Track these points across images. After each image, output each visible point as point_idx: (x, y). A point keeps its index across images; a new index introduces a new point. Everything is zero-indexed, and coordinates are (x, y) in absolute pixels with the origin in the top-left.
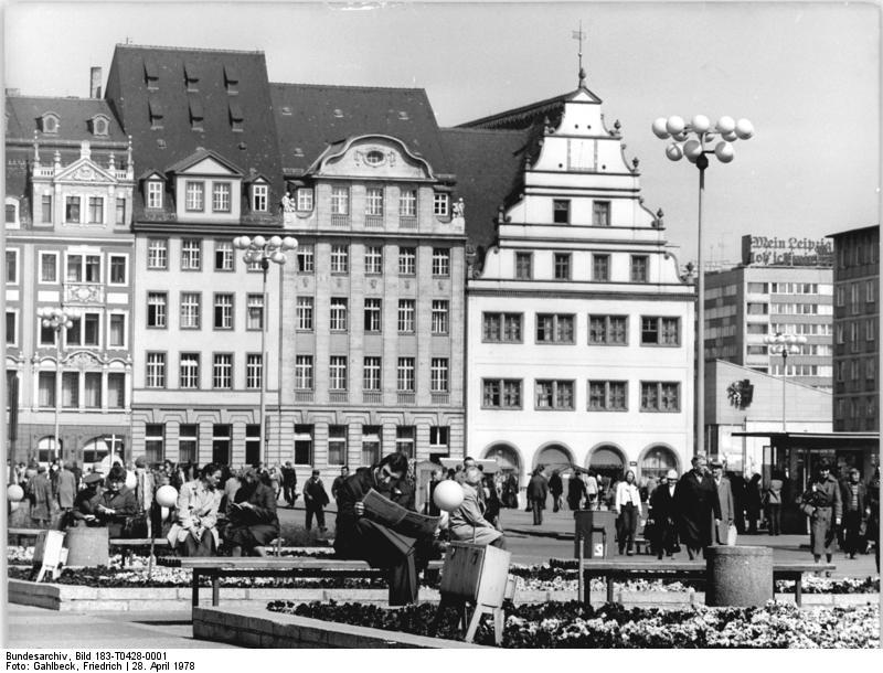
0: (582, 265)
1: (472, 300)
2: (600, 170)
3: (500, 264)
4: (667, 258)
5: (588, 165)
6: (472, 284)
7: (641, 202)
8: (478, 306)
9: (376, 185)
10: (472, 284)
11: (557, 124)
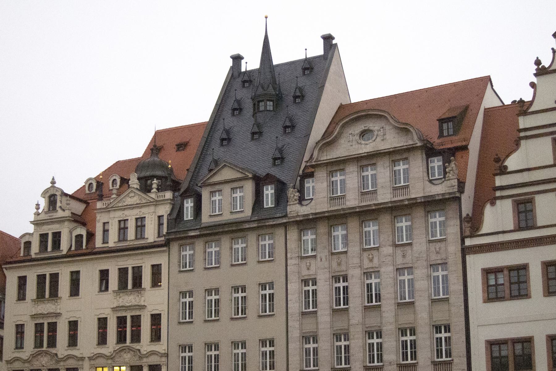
1: (470, 259)
3: (498, 217)
6: (468, 242)
8: (477, 263)
10: (468, 242)
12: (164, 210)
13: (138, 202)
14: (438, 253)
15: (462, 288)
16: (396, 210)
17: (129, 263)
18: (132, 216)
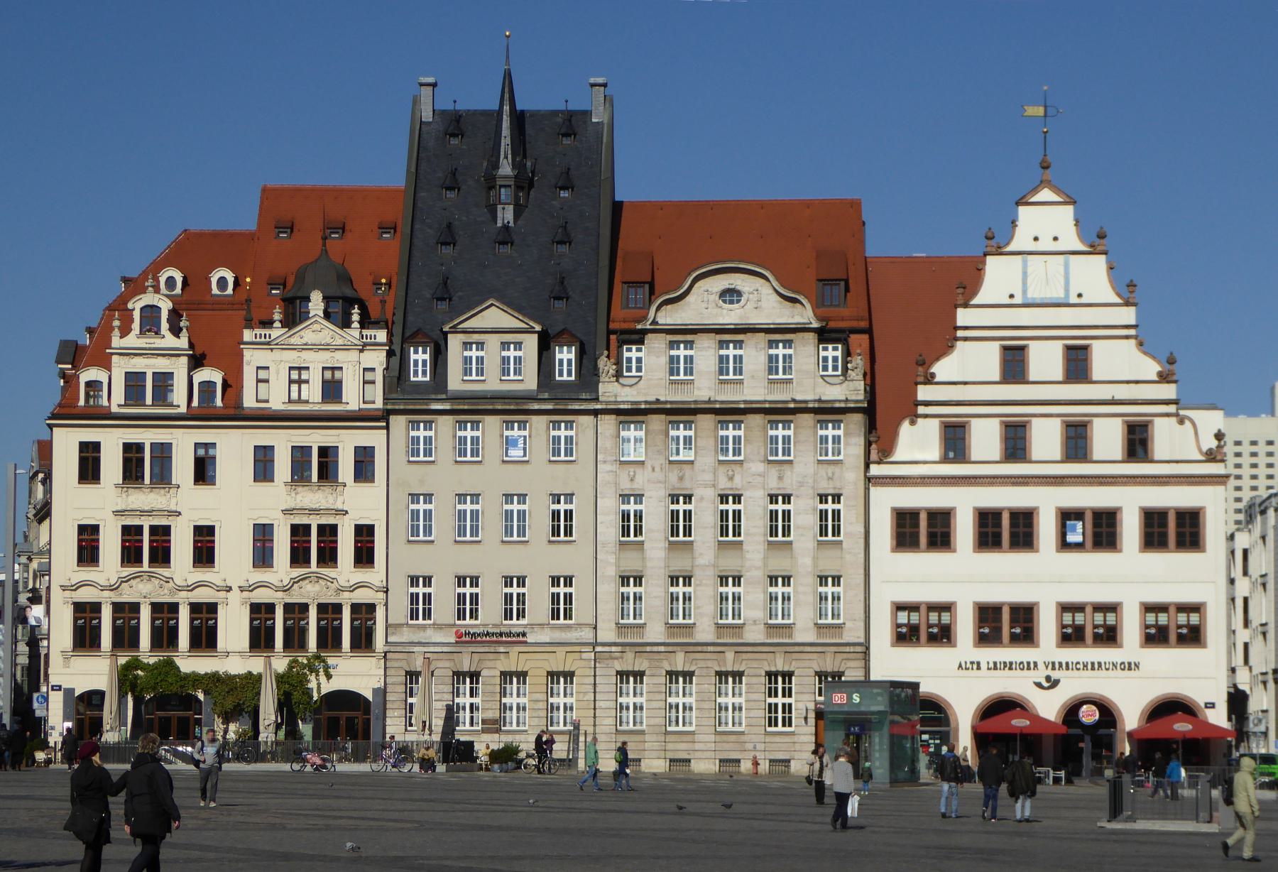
0: (1046, 439)
1: (875, 492)
2: (1074, 300)
3: (918, 443)
4: (1181, 422)
5: (1057, 293)
6: (875, 470)
7: (1141, 344)
10: (875, 470)
12: (377, 359)
13: (329, 340)
14: (829, 479)
15: (862, 530)
16: (779, 412)
17: (315, 438)
18: (316, 362)
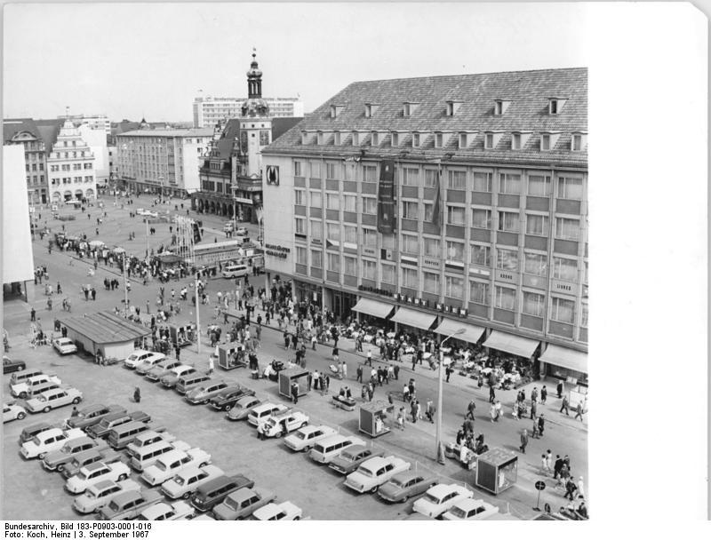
3: (53, 155)
9: (25, 142)
11: (63, 126)
